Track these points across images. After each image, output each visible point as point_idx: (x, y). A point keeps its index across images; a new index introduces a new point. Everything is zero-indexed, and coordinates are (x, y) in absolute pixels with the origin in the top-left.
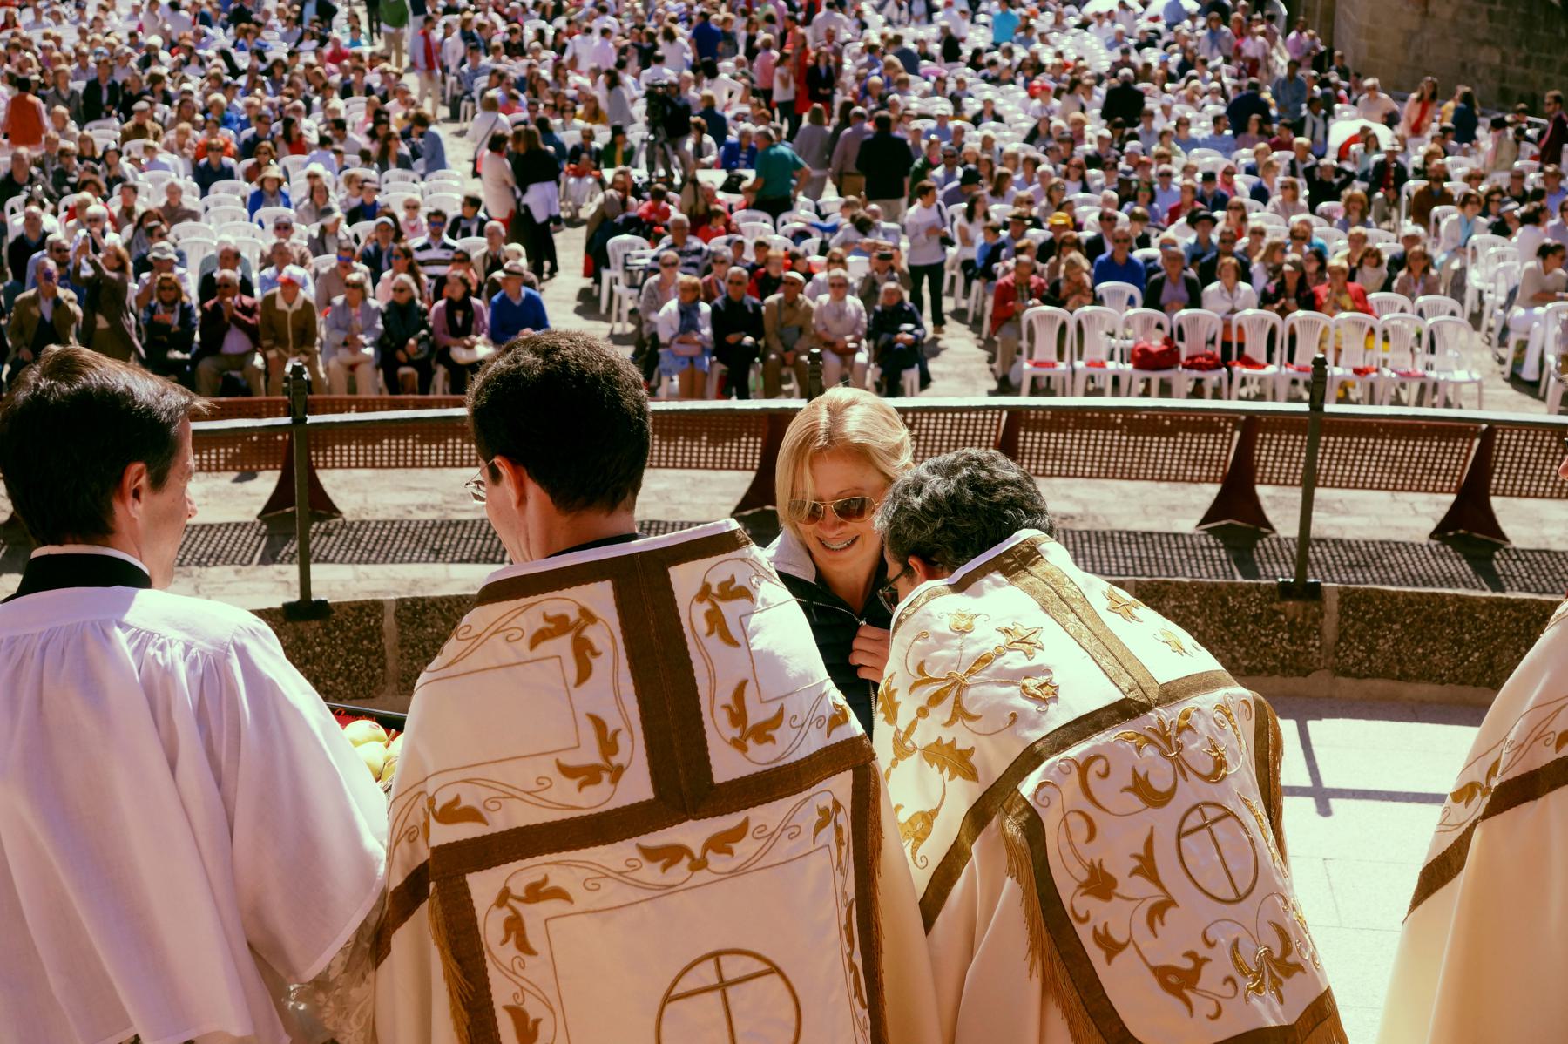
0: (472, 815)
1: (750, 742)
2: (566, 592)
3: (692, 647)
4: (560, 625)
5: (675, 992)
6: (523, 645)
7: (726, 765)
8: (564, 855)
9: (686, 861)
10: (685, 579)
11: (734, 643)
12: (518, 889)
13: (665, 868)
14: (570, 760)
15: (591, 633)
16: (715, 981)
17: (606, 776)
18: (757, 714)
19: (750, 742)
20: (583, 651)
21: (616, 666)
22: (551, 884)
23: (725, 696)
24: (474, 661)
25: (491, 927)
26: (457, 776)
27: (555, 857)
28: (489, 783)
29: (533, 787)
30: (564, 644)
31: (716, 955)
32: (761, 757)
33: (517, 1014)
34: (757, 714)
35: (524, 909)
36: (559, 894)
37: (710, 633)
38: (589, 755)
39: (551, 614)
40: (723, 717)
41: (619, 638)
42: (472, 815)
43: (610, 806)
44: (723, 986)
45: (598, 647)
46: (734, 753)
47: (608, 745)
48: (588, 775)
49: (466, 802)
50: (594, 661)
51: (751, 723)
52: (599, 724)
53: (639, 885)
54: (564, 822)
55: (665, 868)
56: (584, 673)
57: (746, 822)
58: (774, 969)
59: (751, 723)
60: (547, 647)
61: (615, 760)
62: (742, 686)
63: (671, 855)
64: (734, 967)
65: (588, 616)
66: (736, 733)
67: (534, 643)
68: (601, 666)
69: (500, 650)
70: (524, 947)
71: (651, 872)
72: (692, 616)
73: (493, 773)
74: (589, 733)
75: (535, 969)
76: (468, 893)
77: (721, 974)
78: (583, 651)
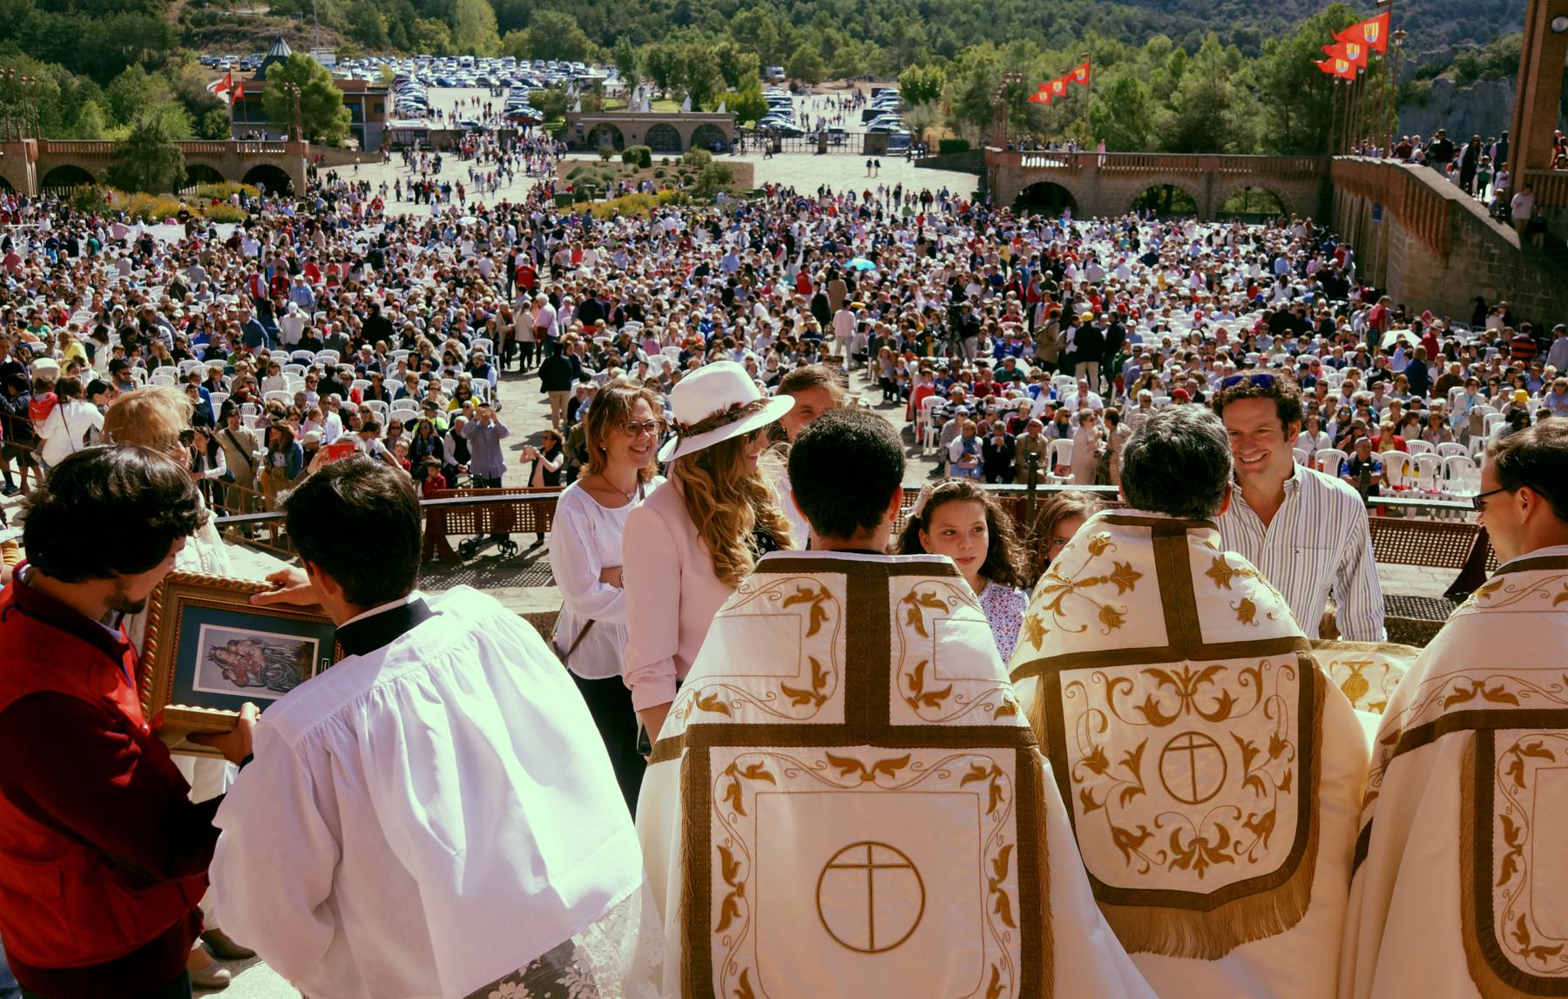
0: (723, 709)
1: (921, 704)
3: (893, 628)
4: (806, 595)
5: (836, 862)
6: (780, 603)
7: (901, 714)
8: (778, 750)
9: (859, 772)
10: (899, 586)
13: (843, 773)
14: (790, 684)
15: (827, 605)
16: (865, 862)
17: (813, 701)
18: (930, 686)
19: (921, 704)
20: (817, 616)
21: (837, 631)
23: (910, 668)
26: (718, 680)
27: (770, 749)
28: (737, 690)
29: (764, 697)
30: (805, 608)
31: (869, 844)
32: (927, 716)
34: (930, 686)
36: (767, 776)
37: (909, 623)
38: (805, 684)
39: (803, 587)
40: (905, 681)
41: (844, 612)
42: (723, 709)
43: (812, 721)
46: (908, 708)
47: (819, 679)
48: (801, 697)
49: (721, 698)
50: (824, 624)
51: (924, 691)
52: (815, 665)
54: (779, 726)
55: (843, 773)
56: (814, 629)
57: (908, 757)
58: (910, 865)
59: (924, 691)
60: (793, 608)
61: (822, 691)
62: (924, 663)
63: (850, 766)
64: (880, 856)
65: (825, 593)
66: (913, 694)
67: (787, 603)
68: (827, 628)
70: (738, 807)
71: (832, 773)
72: (899, 610)
73: (740, 683)
74: (807, 668)
75: (742, 825)
76: (708, 759)
77: (869, 858)
78: (817, 616)
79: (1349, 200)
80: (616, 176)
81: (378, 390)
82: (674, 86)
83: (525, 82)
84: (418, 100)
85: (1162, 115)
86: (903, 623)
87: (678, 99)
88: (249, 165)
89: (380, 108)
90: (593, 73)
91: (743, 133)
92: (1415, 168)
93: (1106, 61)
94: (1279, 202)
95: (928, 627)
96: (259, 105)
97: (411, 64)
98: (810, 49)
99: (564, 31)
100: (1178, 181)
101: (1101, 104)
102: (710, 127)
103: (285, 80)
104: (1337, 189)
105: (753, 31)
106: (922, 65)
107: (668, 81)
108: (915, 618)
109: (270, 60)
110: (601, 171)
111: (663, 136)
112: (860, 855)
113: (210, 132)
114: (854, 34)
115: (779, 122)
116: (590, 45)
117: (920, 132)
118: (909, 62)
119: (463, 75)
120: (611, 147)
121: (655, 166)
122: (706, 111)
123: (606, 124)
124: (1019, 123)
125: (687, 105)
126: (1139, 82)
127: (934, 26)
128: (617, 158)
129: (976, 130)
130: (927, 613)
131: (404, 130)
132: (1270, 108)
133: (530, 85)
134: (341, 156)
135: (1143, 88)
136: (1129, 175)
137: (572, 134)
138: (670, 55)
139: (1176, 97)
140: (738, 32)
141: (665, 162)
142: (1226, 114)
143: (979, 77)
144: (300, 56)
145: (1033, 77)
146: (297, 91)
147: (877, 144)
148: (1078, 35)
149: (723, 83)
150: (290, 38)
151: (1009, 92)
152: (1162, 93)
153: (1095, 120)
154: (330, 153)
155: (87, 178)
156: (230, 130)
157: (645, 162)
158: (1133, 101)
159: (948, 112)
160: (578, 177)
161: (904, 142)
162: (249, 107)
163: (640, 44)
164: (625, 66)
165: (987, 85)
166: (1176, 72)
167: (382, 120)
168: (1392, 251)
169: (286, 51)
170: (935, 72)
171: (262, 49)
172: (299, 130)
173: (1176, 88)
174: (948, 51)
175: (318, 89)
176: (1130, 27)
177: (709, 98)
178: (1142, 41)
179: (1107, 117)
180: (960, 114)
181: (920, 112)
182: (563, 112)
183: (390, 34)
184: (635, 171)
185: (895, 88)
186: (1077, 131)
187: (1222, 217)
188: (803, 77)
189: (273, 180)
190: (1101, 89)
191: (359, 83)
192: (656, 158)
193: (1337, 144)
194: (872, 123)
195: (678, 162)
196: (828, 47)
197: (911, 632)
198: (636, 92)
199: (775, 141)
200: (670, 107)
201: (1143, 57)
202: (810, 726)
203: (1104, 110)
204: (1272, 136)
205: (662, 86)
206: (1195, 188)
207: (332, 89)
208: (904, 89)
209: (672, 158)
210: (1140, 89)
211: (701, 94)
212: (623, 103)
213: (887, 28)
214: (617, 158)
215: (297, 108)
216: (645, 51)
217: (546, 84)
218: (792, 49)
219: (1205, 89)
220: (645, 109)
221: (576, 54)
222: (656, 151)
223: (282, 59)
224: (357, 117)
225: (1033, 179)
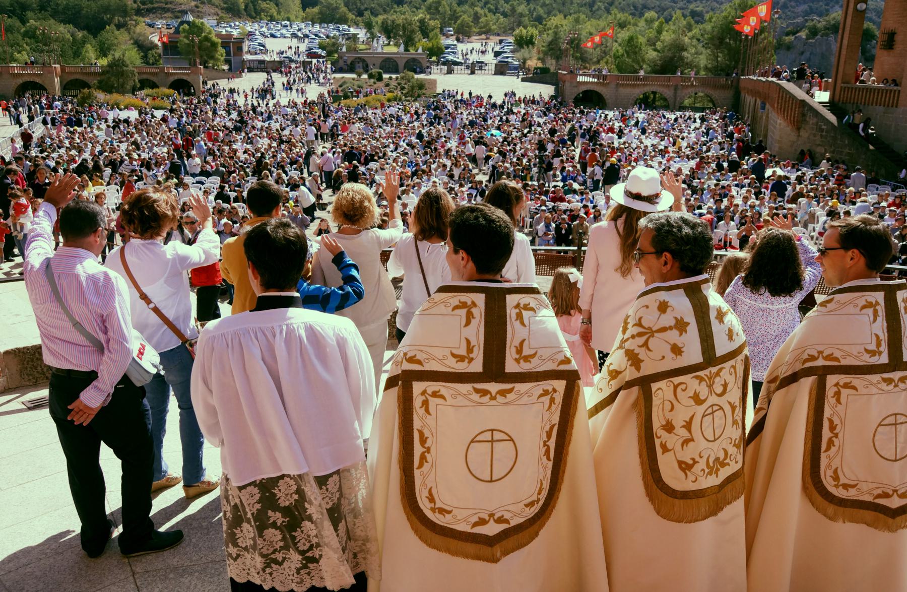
1: (522, 361)
2: (468, 295)
3: (508, 323)
4: (463, 305)
5: (476, 439)
6: (450, 309)
8: (447, 384)
9: (489, 396)
11: (523, 324)
12: (429, 391)
14: (455, 352)
15: (474, 310)
17: (467, 360)
18: (526, 352)
19: (522, 361)
20: (469, 317)
22: (441, 393)
23: (516, 343)
24: (433, 311)
25: (418, 401)
27: (444, 384)
30: (463, 312)
31: (492, 430)
32: (525, 367)
33: (421, 433)
34: (526, 352)
35: (431, 399)
36: (443, 397)
38: (463, 351)
40: (514, 350)
42: (419, 362)
43: (466, 371)
44: (492, 441)
45: (475, 315)
46: (516, 364)
47: (470, 349)
48: (461, 358)
49: (418, 357)
50: (473, 320)
52: (468, 342)
53: (470, 400)
56: (468, 323)
60: (458, 311)
61: (471, 356)
62: (524, 340)
63: (485, 393)
64: (497, 436)
65: (474, 304)
66: (517, 356)
67: (453, 309)
68: (474, 322)
69: (442, 309)
70: (427, 411)
71: (476, 397)
72: (511, 312)
75: (430, 420)
77: (492, 437)
78: (469, 317)
79: (749, 100)
80: (365, 86)
81: (240, 197)
82: (395, 38)
83: (316, 35)
84: (260, 45)
85: (652, 54)
86: (513, 320)
87: (397, 45)
88: (172, 79)
89: (240, 49)
90: (353, 30)
91: (431, 63)
92: (784, 83)
93: (622, 25)
94: (712, 101)
95: (526, 321)
96: (177, 47)
97: (256, 26)
98: (466, 18)
99: (337, 8)
100: (659, 90)
101: (619, 48)
102: (414, 60)
103: (189, 34)
104: (742, 94)
105: (437, 9)
106: (525, 27)
107: (392, 35)
108: (519, 317)
109: (182, 23)
110: (356, 83)
111: (389, 65)
112: (488, 436)
113: (151, 61)
114: (490, 10)
115: (450, 57)
116: (351, 16)
117: (524, 63)
118: (519, 25)
119: (284, 31)
120: (362, 70)
121: (385, 81)
122: (412, 51)
123: (359, 58)
124: (576, 58)
125: (402, 47)
126: (640, 37)
127: (532, 6)
128: (365, 76)
129: (554, 62)
130: (526, 314)
131: (253, 61)
132: (708, 51)
133: (320, 37)
134: (220, 74)
135: (642, 40)
136: (634, 86)
137: (341, 63)
138: (393, 22)
139: (659, 45)
140: (429, 8)
141: (390, 78)
142: (685, 54)
143: (556, 33)
144: (198, 21)
145: (584, 33)
146: (197, 40)
147: (502, 69)
148: (608, 11)
149: (420, 36)
150: (192, 11)
151: (571, 42)
152: (652, 43)
153: (616, 57)
154: (214, 73)
155: (86, 85)
156: (161, 61)
157: (380, 79)
158: (636, 47)
159: (539, 52)
160: (344, 86)
161: (516, 68)
162: (171, 48)
163: (376, 15)
164: (369, 26)
165: (559, 38)
166: (659, 32)
167: (241, 55)
168: (770, 127)
169: (191, 18)
170: (533, 31)
171: (177, 17)
172: (198, 61)
173: (659, 40)
174: (539, 20)
175: (207, 39)
176: (635, 8)
177: (414, 44)
178: (641, 15)
179: (623, 55)
180: (545, 53)
181: (524, 52)
182: (336, 51)
183: (245, 10)
184: (375, 83)
185: (511, 39)
186: (607, 63)
187: (682, 108)
188: (463, 33)
189: (182, 86)
190: (619, 40)
191: (229, 36)
192: (386, 76)
193: (743, 70)
194: (499, 58)
195: (397, 78)
196: (476, 17)
197: (517, 324)
198: (375, 40)
199: (450, 66)
200: (392, 49)
201: (642, 23)
202: (465, 373)
203: (621, 51)
204: (709, 66)
205: (389, 38)
206: (668, 93)
207: (215, 39)
208: (516, 40)
209: (394, 76)
210: (640, 41)
211: (409, 42)
212: (368, 47)
213: (507, 8)
214: (365, 76)
215: (196, 49)
216: (380, 19)
217: (328, 37)
218: (457, 18)
219: (675, 41)
220: (379, 50)
221: (343, 20)
222: (386, 72)
223: (188, 23)
224: (228, 53)
225: (584, 88)
